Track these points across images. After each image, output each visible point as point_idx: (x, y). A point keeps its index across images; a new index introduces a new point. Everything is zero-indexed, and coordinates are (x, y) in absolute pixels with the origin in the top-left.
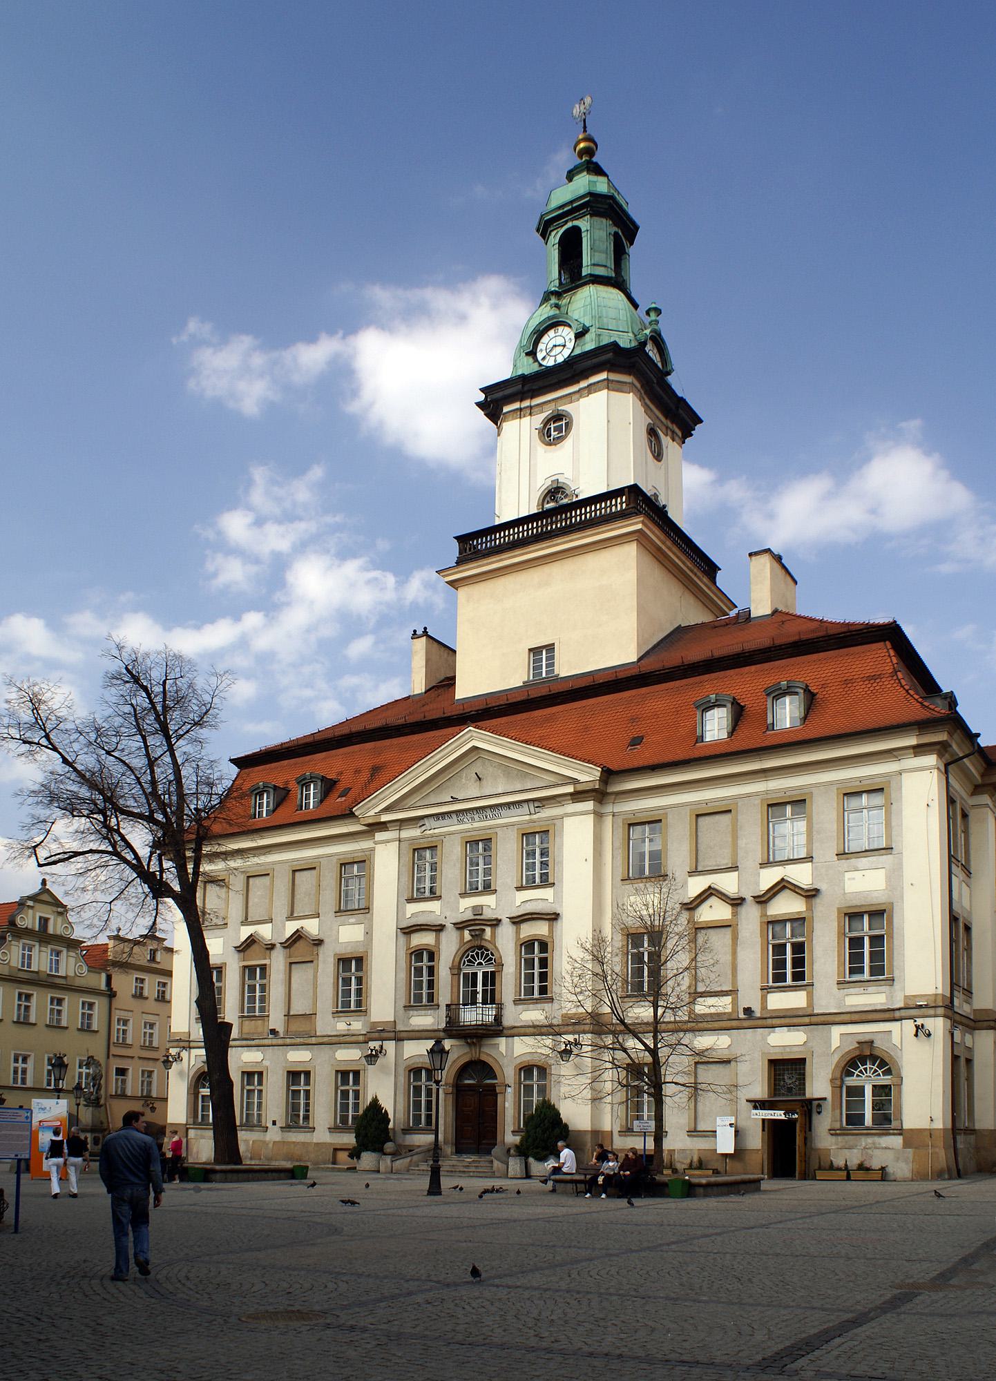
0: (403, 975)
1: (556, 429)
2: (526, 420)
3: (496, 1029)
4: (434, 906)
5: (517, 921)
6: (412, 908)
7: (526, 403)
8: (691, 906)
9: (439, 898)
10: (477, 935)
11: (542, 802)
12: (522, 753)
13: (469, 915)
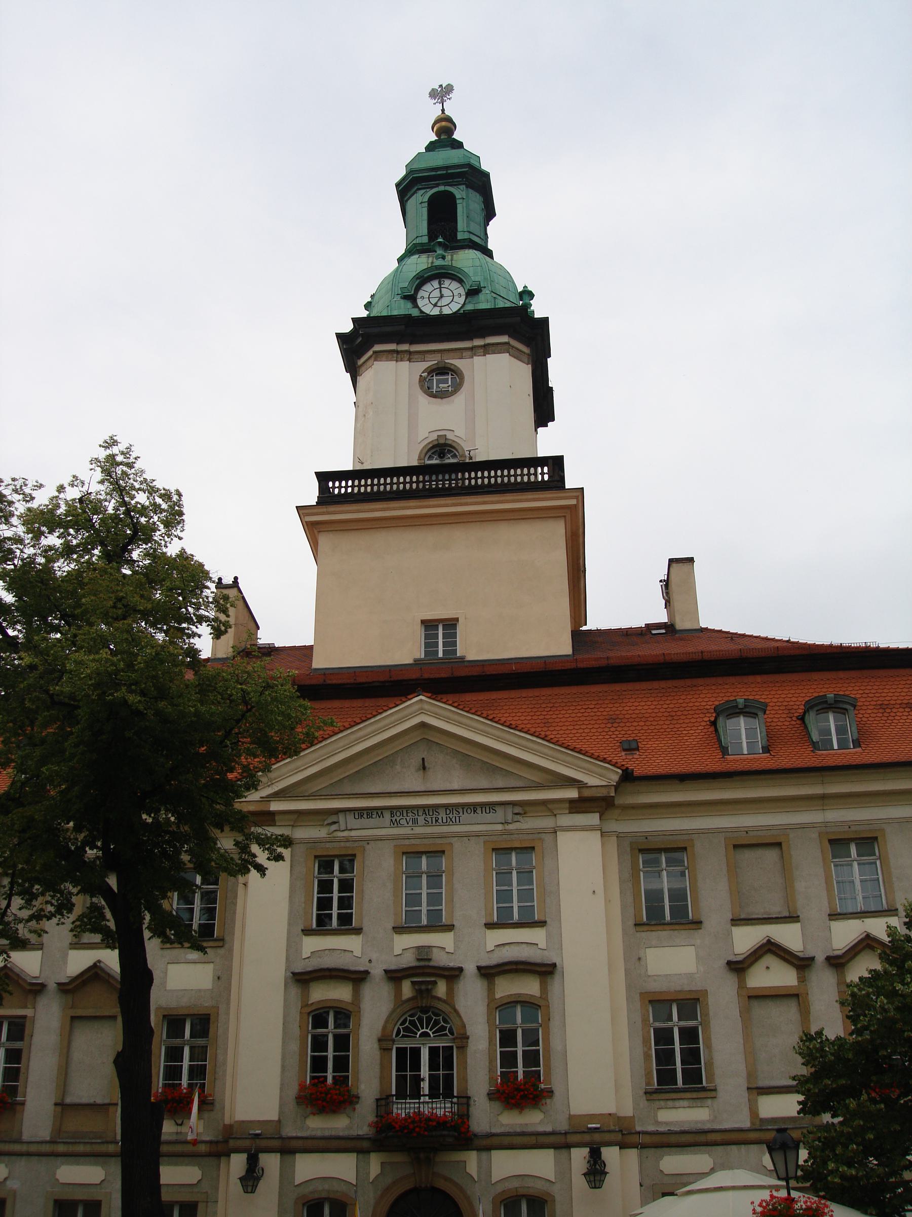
0: (295, 1047)
1: (442, 381)
2: (405, 365)
3: (459, 1135)
4: (350, 944)
5: (488, 973)
6: (311, 944)
7: (405, 347)
8: (739, 967)
9: (358, 931)
10: (424, 991)
11: (522, 809)
12: (498, 739)
13: (409, 960)
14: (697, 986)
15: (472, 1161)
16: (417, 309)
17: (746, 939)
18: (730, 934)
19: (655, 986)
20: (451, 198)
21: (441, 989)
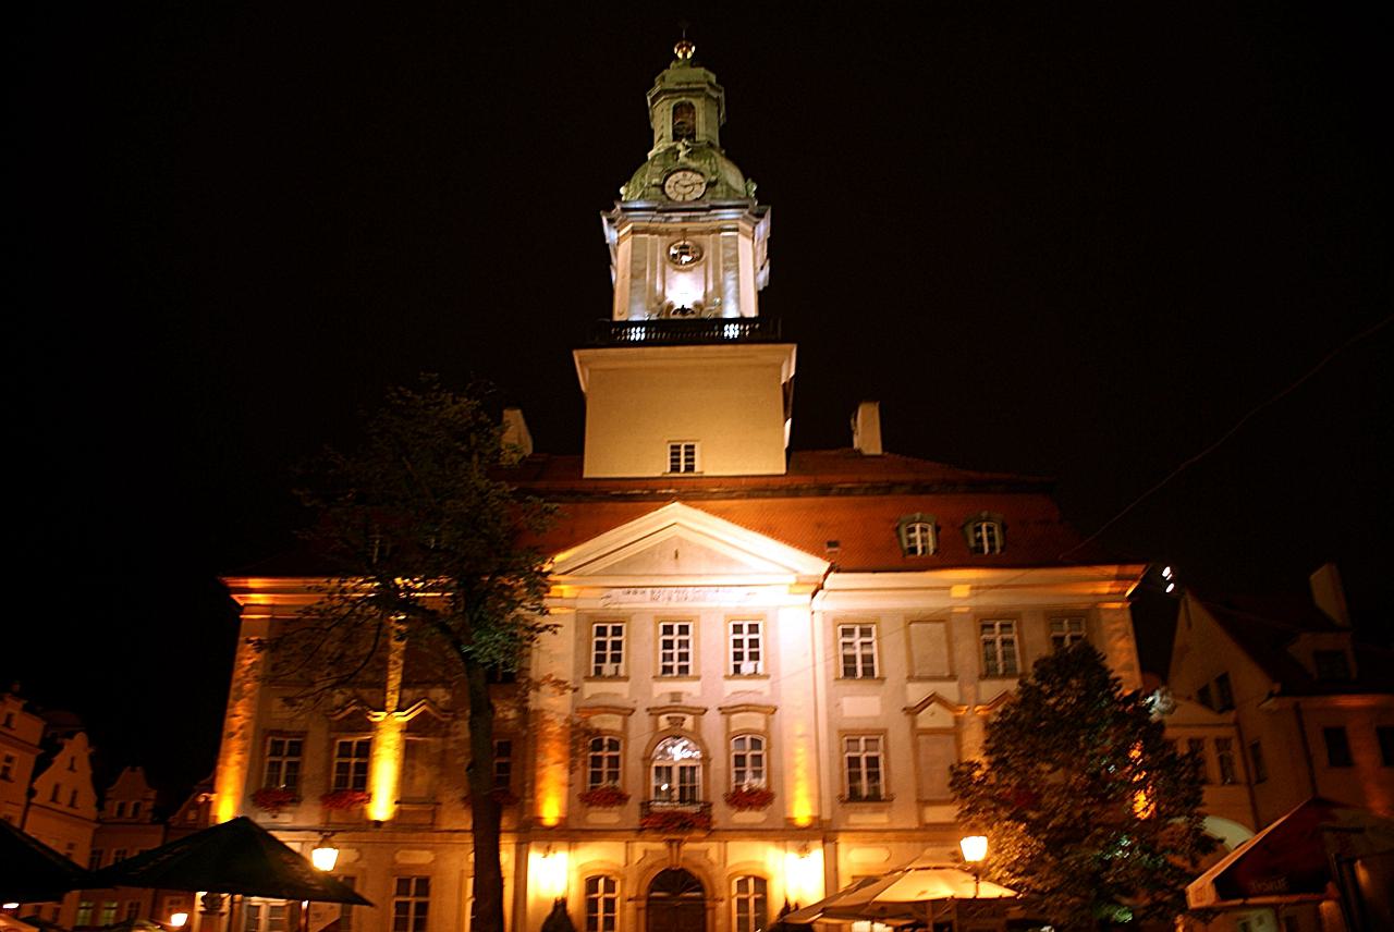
5: (726, 711)
8: (912, 712)
9: (626, 679)
13: (666, 701)
14: (881, 726)
15: (713, 849)
16: (664, 197)
17: (916, 693)
18: (904, 689)
19: (847, 725)
20: (691, 107)
21: (689, 722)
